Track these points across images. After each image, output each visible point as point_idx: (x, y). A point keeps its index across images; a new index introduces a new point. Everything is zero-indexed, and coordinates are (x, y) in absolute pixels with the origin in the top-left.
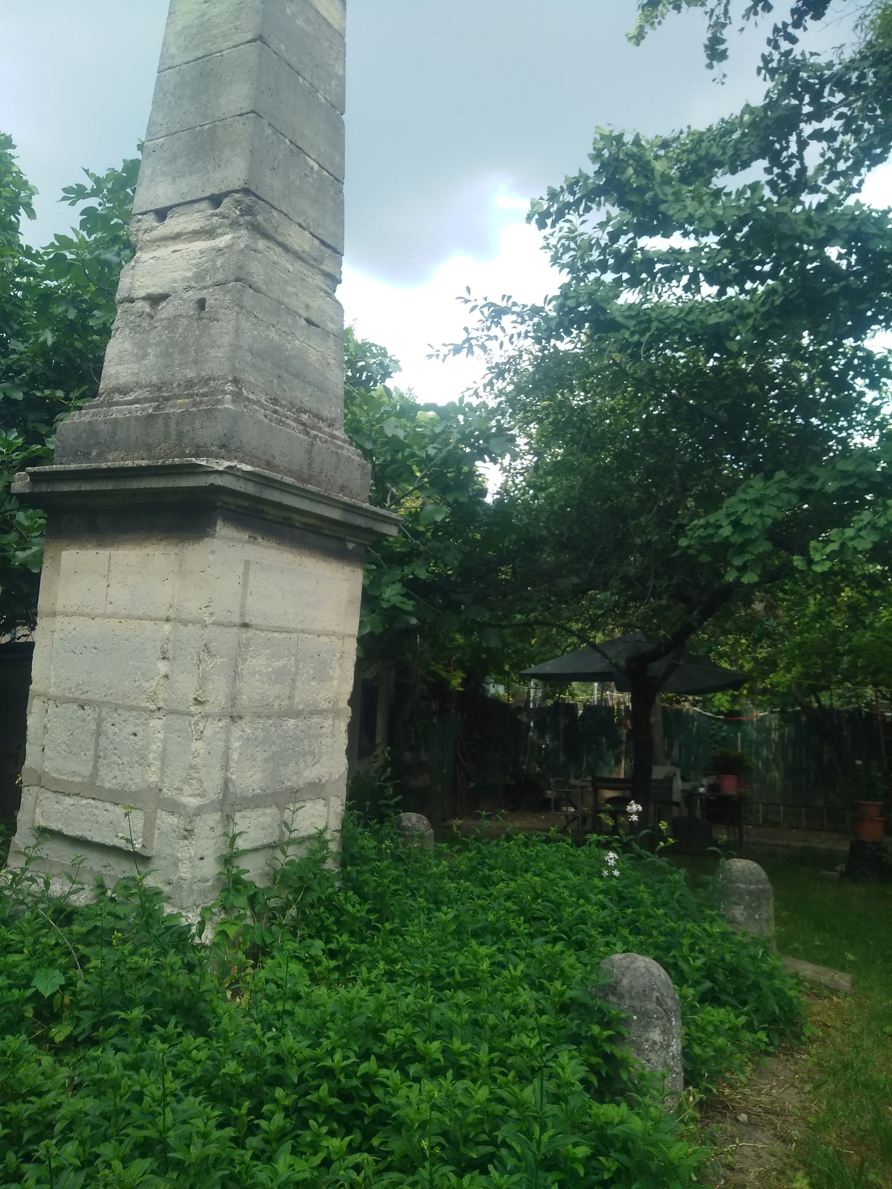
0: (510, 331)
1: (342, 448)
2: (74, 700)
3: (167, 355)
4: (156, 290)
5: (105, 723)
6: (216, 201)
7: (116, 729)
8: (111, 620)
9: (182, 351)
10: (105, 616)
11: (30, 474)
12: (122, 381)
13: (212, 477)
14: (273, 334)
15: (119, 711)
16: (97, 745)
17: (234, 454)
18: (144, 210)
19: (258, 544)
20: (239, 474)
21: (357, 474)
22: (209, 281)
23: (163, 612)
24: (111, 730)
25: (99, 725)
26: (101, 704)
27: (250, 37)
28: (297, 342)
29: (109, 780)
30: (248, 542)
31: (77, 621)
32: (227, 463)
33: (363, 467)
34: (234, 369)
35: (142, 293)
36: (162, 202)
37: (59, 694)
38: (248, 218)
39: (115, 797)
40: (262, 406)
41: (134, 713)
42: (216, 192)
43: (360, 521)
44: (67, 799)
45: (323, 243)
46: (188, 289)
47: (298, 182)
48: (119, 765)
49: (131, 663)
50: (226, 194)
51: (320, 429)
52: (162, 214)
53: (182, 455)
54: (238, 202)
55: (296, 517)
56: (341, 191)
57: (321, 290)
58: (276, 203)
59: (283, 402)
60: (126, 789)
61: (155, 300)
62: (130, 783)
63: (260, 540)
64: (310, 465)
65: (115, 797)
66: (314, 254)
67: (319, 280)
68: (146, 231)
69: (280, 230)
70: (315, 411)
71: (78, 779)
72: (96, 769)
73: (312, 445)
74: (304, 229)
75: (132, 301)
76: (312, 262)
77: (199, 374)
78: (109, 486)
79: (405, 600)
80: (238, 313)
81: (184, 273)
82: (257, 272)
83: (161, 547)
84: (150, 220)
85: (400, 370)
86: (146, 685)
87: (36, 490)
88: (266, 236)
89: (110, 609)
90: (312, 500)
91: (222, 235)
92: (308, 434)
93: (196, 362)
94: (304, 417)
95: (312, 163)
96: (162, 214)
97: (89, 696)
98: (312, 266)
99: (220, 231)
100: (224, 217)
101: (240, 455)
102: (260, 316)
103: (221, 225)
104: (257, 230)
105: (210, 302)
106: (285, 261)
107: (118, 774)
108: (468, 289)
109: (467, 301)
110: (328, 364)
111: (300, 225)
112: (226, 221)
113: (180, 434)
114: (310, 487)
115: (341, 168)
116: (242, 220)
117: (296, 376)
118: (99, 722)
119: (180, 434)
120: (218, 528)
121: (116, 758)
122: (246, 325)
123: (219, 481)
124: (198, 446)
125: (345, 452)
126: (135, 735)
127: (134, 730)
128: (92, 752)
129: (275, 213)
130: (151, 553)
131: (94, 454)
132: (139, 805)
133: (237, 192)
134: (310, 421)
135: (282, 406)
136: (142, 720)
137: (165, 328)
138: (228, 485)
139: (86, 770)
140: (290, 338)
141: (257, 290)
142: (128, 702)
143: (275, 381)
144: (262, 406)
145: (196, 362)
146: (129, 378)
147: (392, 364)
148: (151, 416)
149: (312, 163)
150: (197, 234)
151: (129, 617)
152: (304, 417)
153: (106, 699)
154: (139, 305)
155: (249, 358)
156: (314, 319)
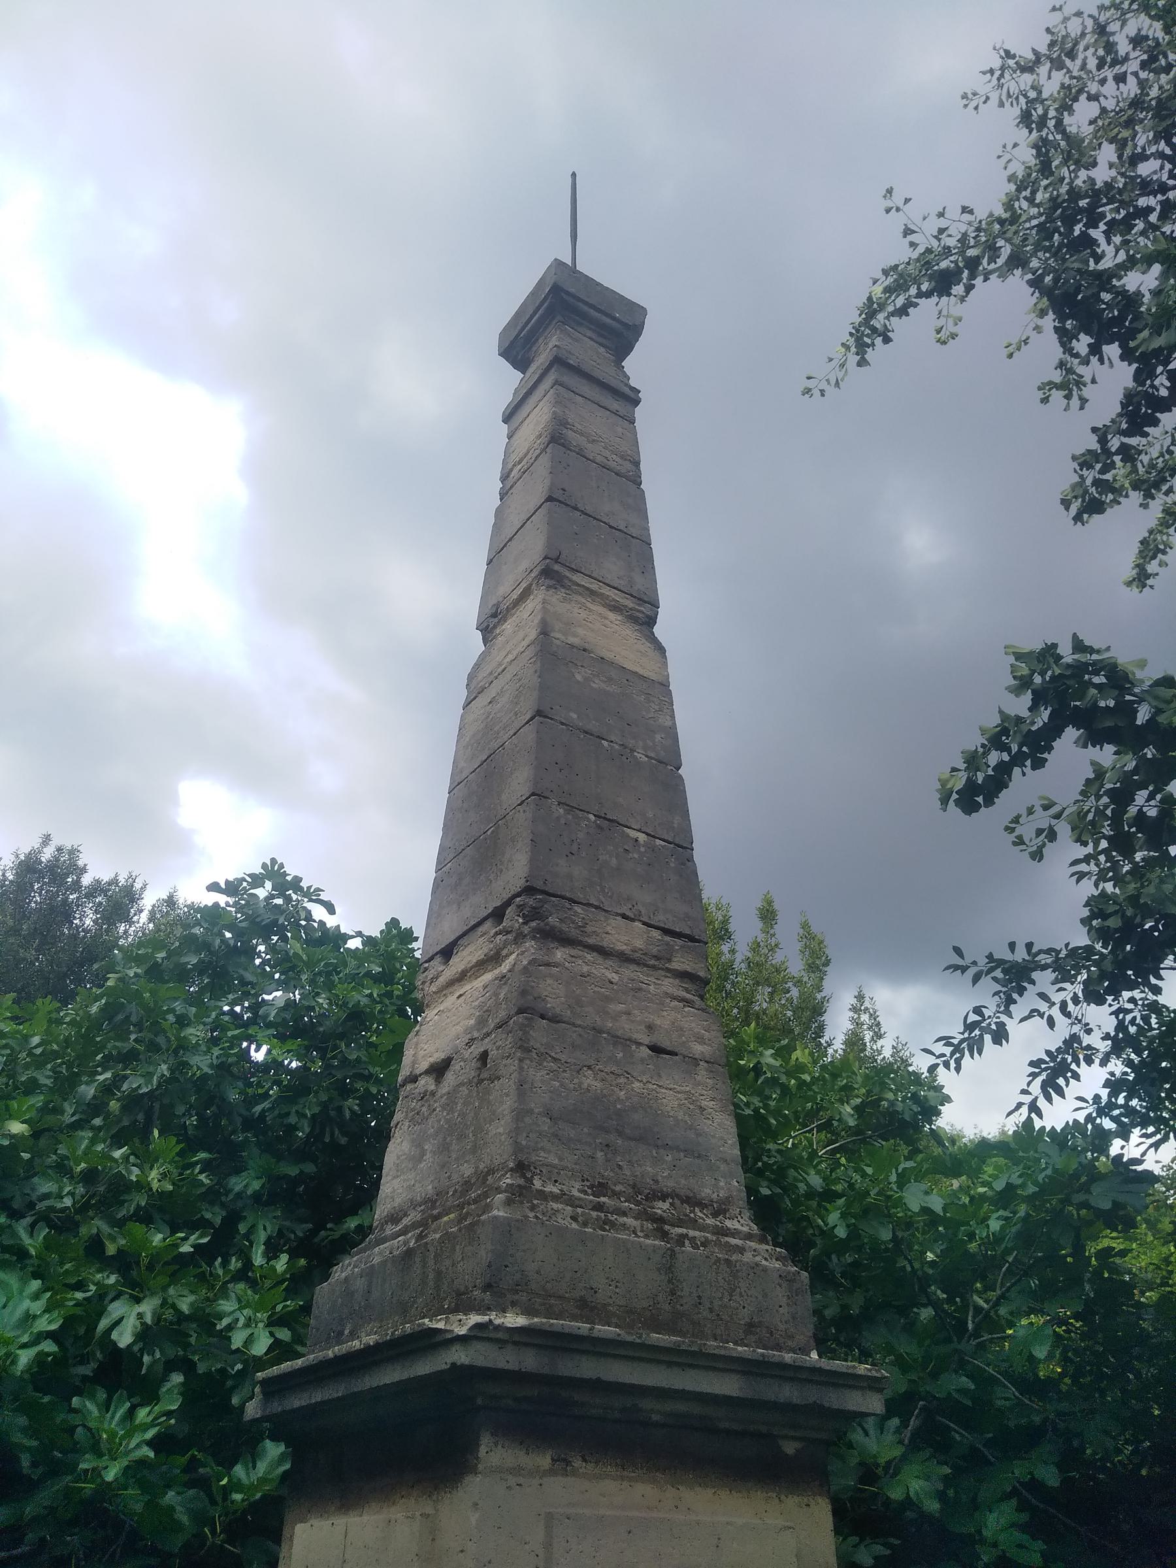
0: (1057, 998)
1: (741, 1250)
3: (444, 1148)
4: (438, 1056)
6: (498, 915)
9: (462, 1137)
11: (264, 1383)
14: (589, 1080)
17: (509, 1297)
19: (575, 1473)
20: (500, 1335)
21: (780, 1295)
22: (492, 1024)
27: (528, 717)
28: (636, 1085)
30: (551, 1472)
32: (475, 1319)
33: (789, 1280)
34: (518, 1148)
35: (424, 1065)
38: (534, 924)
40: (571, 1202)
43: (788, 1393)
45: (666, 932)
47: (614, 861)
50: (508, 903)
51: (694, 1224)
52: (447, 953)
54: (520, 907)
55: (647, 1404)
56: (690, 859)
57: (674, 998)
58: (580, 896)
59: (618, 1188)
61: (439, 1070)
63: (578, 1463)
64: (673, 1293)
66: (655, 951)
67: (670, 985)
69: (589, 929)
70: (682, 1193)
73: (673, 1254)
74: (633, 920)
76: (652, 962)
78: (333, 1391)
79: (1025, 1538)
80: (521, 1060)
82: (553, 994)
84: (437, 965)
85: (947, 1099)
88: (566, 941)
90: (670, 1364)
91: (507, 956)
92: (664, 1235)
93: (475, 1149)
94: (661, 1207)
95: (633, 834)
96: (447, 953)
98: (654, 967)
99: (504, 952)
100: (508, 933)
101: (523, 1297)
102: (563, 1057)
104: (550, 936)
105: (493, 1053)
106: (606, 971)
108: (958, 951)
109: (964, 969)
110: (702, 1109)
111: (624, 917)
112: (510, 937)
114: (656, 1338)
115: (687, 830)
116: (526, 929)
117: (640, 1139)
120: (483, 1450)
122: (538, 1076)
123: (460, 1356)
124: (459, 1294)
125: (748, 1257)
129: (578, 909)
131: (346, 1332)
133: (518, 895)
134: (667, 1212)
135: (616, 1195)
138: (480, 1362)
140: (622, 1080)
141: (555, 1020)
143: (599, 1154)
144: (571, 1202)
147: (931, 1094)
148: (409, 1254)
149: (633, 834)
152: (661, 1207)
154: (422, 1081)
155: (545, 1125)
156: (666, 1044)
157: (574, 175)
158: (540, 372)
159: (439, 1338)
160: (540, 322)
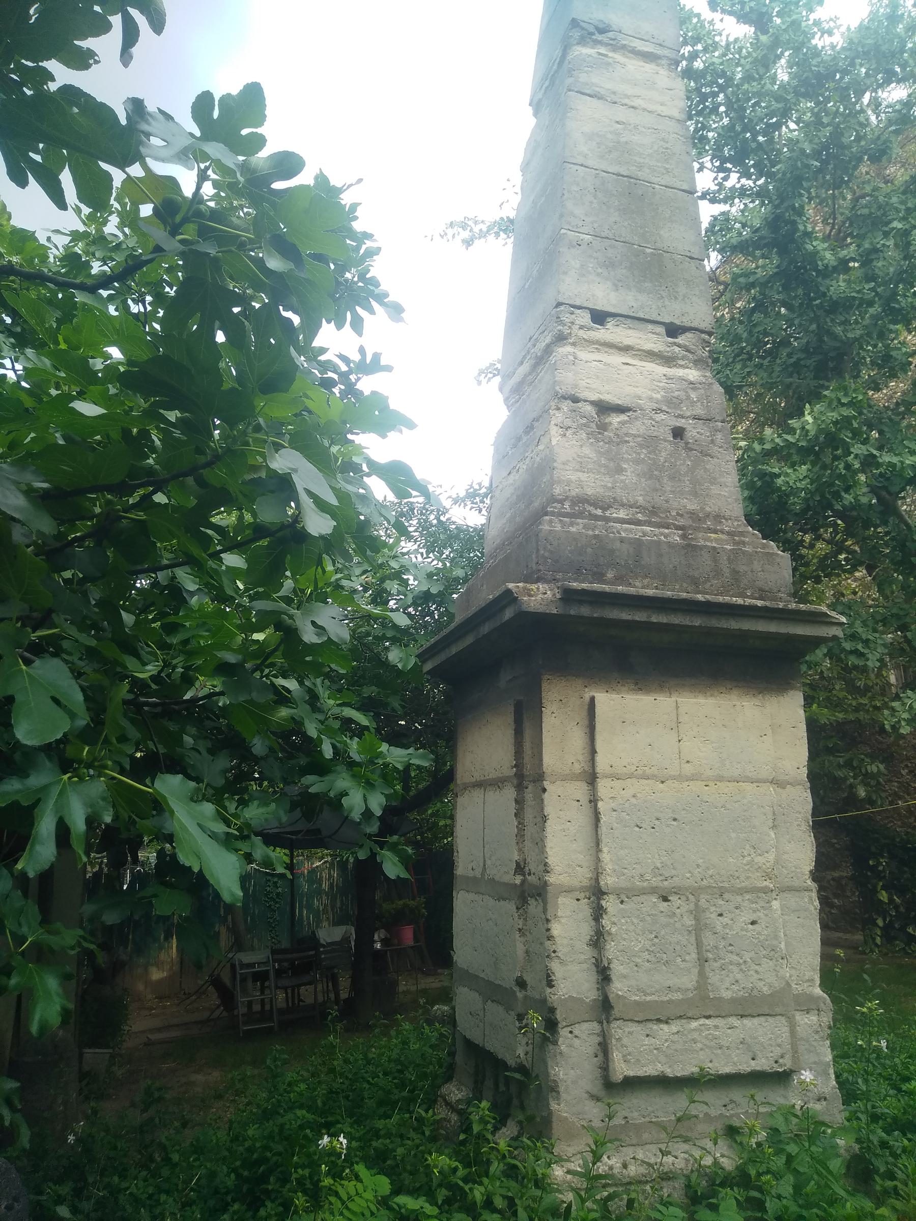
2: (653, 891)
5: (708, 915)
6: (673, 331)
7: (724, 920)
8: (691, 783)
10: (680, 778)
12: (590, 491)
13: (835, 628)
15: (726, 896)
16: (699, 945)
18: (578, 303)
23: (766, 772)
24: (719, 923)
25: (697, 919)
26: (696, 891)
29: (725, 986)
31: (633, 787)
35: (594, 397)
36: (602, 305)
37: (623, 884)
39: (748, 1007)
41: (747, 897)
42: (678, 322)
44: (665, 1027)
46: (658, 410)
48: (739, 964)
49: (733, 835)
50: (684, 330)
52: (600, 317)
53: (743, 595)
60: (755, 993)
61: (604, 408)
62: (760, 984)
65: (748, 1007)
68: (581, 327)
71: (677, 996)
72: (702, 974)
75: (576, 400)
77: (702, 509)
81: (650, 393)
84: (585, 318)
86: (759, 859)
89: (688, 769)
96: (600, 317)
97: (676, 881)
100: (688, 351)
103: (683, 358)
107: (739, 976)
112: (691, 356)
113: (735, 572)
118: (697, 913)
119: (735, 572)
121: (735, 958)
124: (761, 590)
126: (753, 923)
127: (753, 917)
128: (694, 956)
130: (738, 703)
132: (778, 1010)
136: (762, 904)
137: (641, 446)
139: (689, 981)
142: (738, 884)
145: (695, 494)
146: (601, 491)
150: (651, 355)
151: (720, 779)
153: (705, 882)
159: (828, 620)
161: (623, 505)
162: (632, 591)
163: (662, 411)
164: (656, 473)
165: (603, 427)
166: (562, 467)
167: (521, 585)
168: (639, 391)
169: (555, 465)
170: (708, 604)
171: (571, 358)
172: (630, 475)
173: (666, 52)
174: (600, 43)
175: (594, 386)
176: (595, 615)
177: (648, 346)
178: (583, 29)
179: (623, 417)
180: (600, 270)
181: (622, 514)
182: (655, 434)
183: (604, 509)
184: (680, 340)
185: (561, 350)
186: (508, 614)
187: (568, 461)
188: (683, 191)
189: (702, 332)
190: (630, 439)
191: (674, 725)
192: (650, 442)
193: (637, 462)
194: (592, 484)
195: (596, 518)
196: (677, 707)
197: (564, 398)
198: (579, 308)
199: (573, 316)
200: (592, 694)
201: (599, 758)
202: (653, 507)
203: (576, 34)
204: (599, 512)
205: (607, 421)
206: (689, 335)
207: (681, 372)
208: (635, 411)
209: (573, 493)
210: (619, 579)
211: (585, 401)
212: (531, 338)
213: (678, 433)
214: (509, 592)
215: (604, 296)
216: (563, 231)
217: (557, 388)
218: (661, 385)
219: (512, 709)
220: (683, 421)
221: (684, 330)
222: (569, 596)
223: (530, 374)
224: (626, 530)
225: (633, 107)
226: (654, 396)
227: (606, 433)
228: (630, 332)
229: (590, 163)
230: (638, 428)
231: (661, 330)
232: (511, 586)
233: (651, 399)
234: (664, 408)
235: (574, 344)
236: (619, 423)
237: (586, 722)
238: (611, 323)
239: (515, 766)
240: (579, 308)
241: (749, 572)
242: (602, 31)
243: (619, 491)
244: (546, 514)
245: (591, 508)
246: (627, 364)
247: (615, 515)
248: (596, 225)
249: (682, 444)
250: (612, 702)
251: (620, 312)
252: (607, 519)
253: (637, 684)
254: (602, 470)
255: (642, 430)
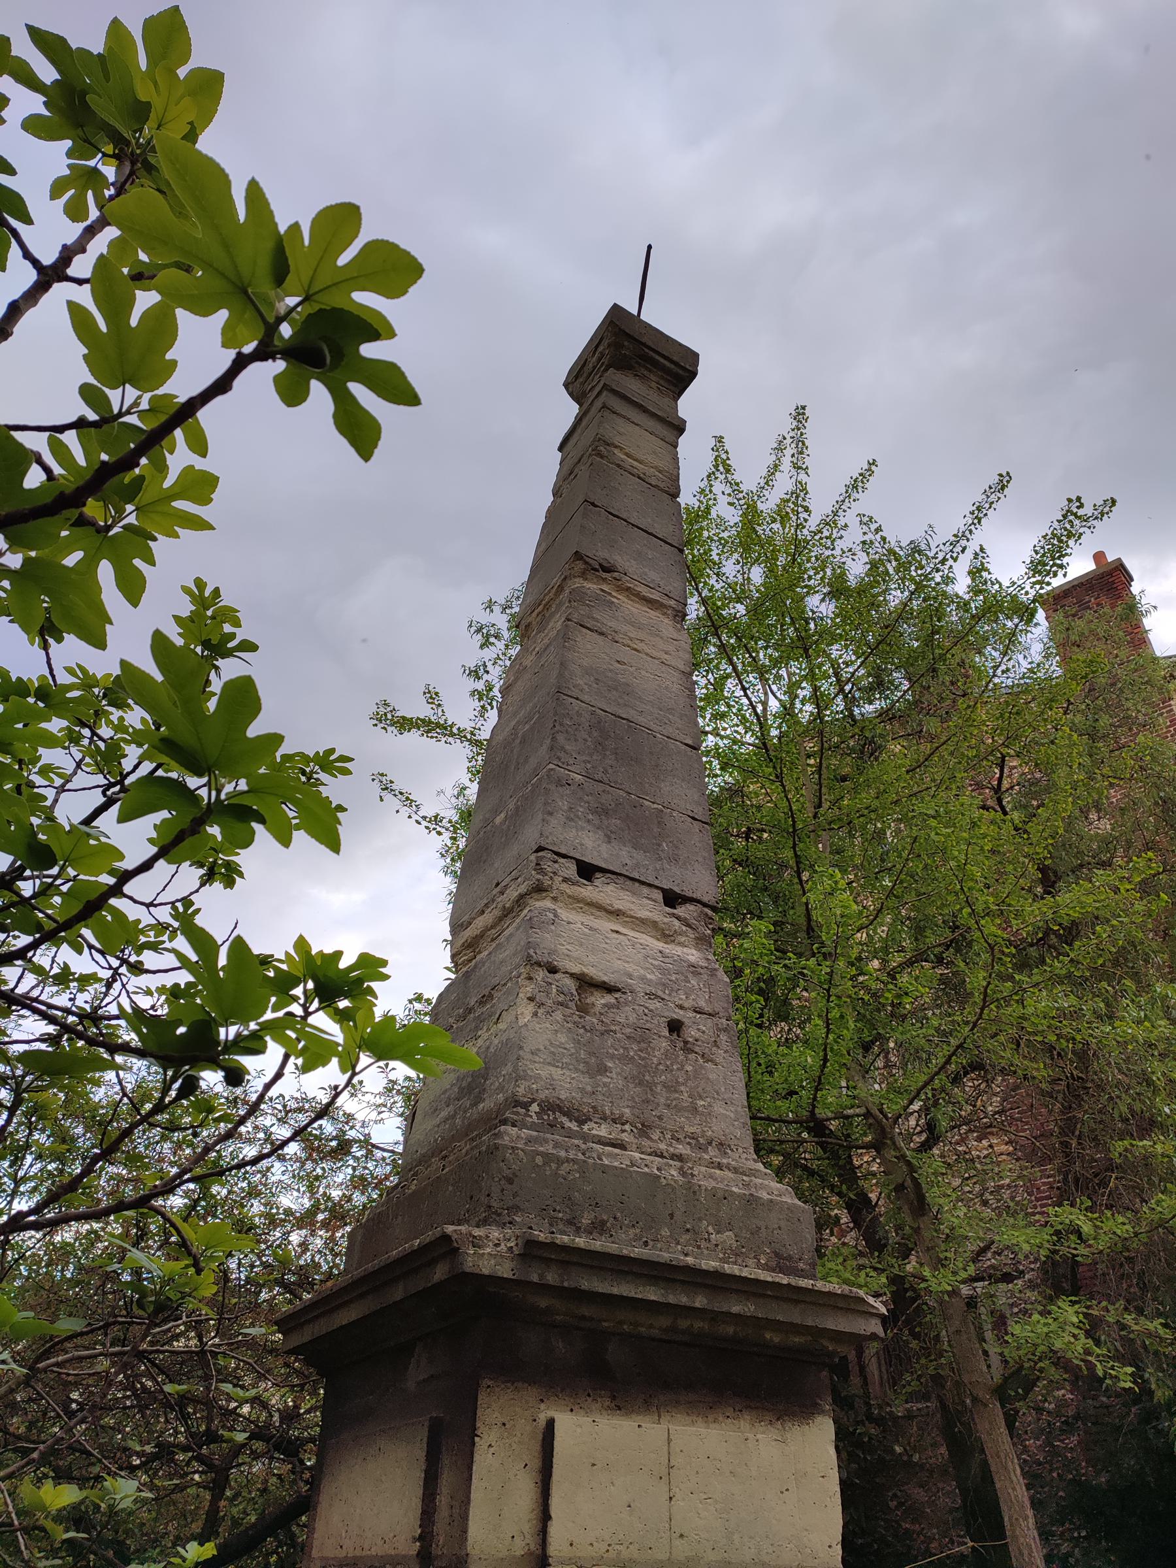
6: (672, 899)
18: (563, 851)
35: (576, 969)
46: (651, 996)
50: (687, 900)
52: (587, 871)
61: (586, 983)
68: (565, 880)
75: (553, 970)
81: (642, 971)
83: (744, 1423)
84: (571, 870)
87: (535, 1278)
96: (587, 871)
130: (751, 1436)
157: (650, 247)
158: (665, 416)
159: (865, 1308)
160: (667, 371)
161: (604, 1118)
162: (612, 1248)
163: (657, 997)
164: (647, 1078)
165: (583, 1009)
166: (530, 1056)
167: (463, 1228)
168: (630, 968)
169: (521, 1052)
170: (717, 1274)
171: (551, 916)
172: (614, 1078)
173: (672, 603)
174: (604, 580)
175: (575, 954)
176: (566, 1284)
177: (644, 914)
178: (586, 563)
179: (609, 999)
180: (590, 817)
181: (603, 1131)
182: (648, 1026)
183: (581, 1123)
184: (680, 911)
185: (538, 904)
186: (440, 1273)
187: (539, 1050)
188: (686, 745)
189: (705, 905)
190: (617, 1028)
191: (664, 1471)
192: (641, 1036)
193: (626, 1059)
194: (566, 1083)
195: (570, 1134)
196: (669, 1441)
197: (539, 964)
198: (564, 856)
199: (556, 865)
200: (551, 1413)
201: (554, 1529)
202: (643, 1125)
203: (580, 566)
204: (574, 1126)
205: (588, 1001)
206: (691, 907)
207: (678, 951)
208: (624, 993)
209: (542, 1096)
210: (599, 1228)
211: (566, 973)
212: (498, 884)
213: (675, 1027)
214: (446, 1238)
215: (593, 847)
216: (551, 766)
217: (531, 951)
218: (656, 963)
219: (423, 1434)
220: (681, 1012)
221: (687, 900)
222: (531, 1251)
223: (492, 927)
224: (609, 1155)
225: (636, 650)
226: (649, 976)
227: (588, 1018)
228: (622, 894)
229: (586, 698)
230: (627, 1015)
231: (659, 896)
232: (450, 1229)
233: (642, 978)
234: (660, 993)
235: (555, 899)
236: (605, 1005)
237: (536, 1463)
238: (599, 879)
239: (421, 1538)
240: (564, 856)
241: (763, 1229)
242: (607, 570)
243: (601, 1097)
244: (504, 1122)
245: (564, 1119)
246: (617, 932)
247: (594, 1132)
248: (589, 766)
249: (680, 1044)
250: (579, 1430)
251: (611, 868)
252: (585, 1138)
253: (613, 1398)
254: (581, 1067)
255: (632, 1018)
